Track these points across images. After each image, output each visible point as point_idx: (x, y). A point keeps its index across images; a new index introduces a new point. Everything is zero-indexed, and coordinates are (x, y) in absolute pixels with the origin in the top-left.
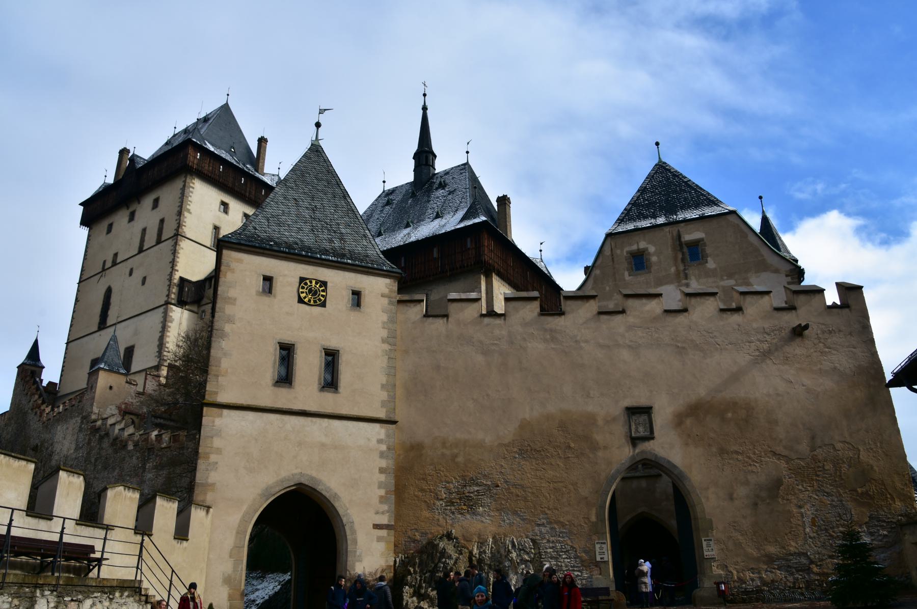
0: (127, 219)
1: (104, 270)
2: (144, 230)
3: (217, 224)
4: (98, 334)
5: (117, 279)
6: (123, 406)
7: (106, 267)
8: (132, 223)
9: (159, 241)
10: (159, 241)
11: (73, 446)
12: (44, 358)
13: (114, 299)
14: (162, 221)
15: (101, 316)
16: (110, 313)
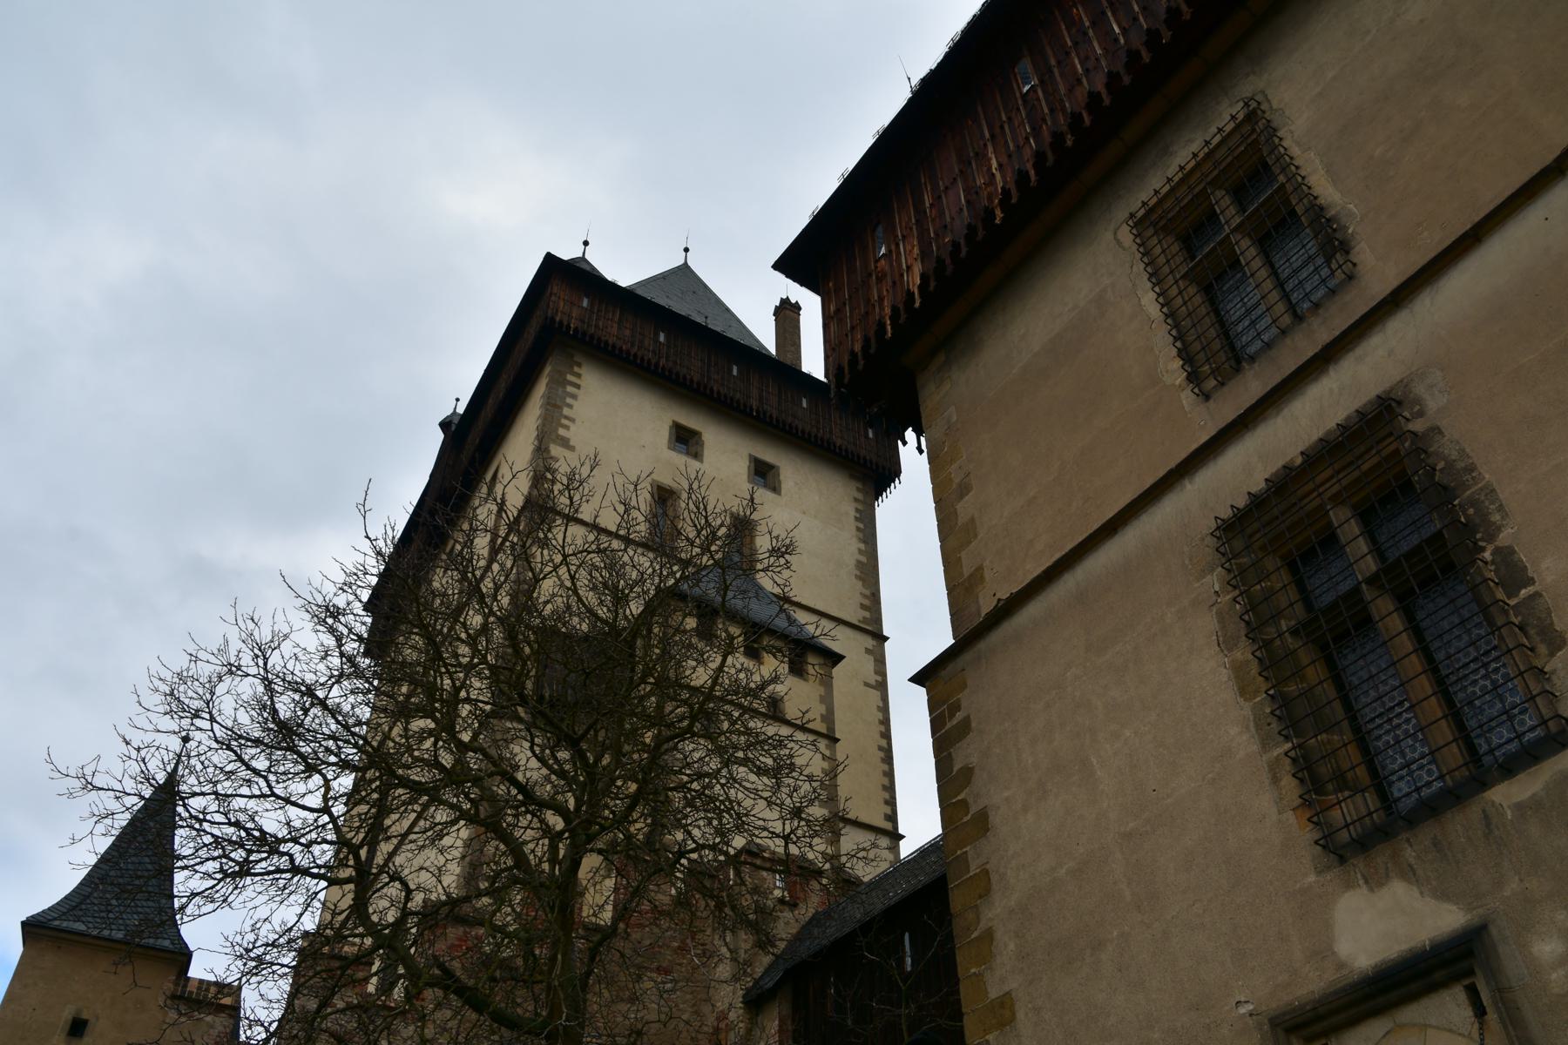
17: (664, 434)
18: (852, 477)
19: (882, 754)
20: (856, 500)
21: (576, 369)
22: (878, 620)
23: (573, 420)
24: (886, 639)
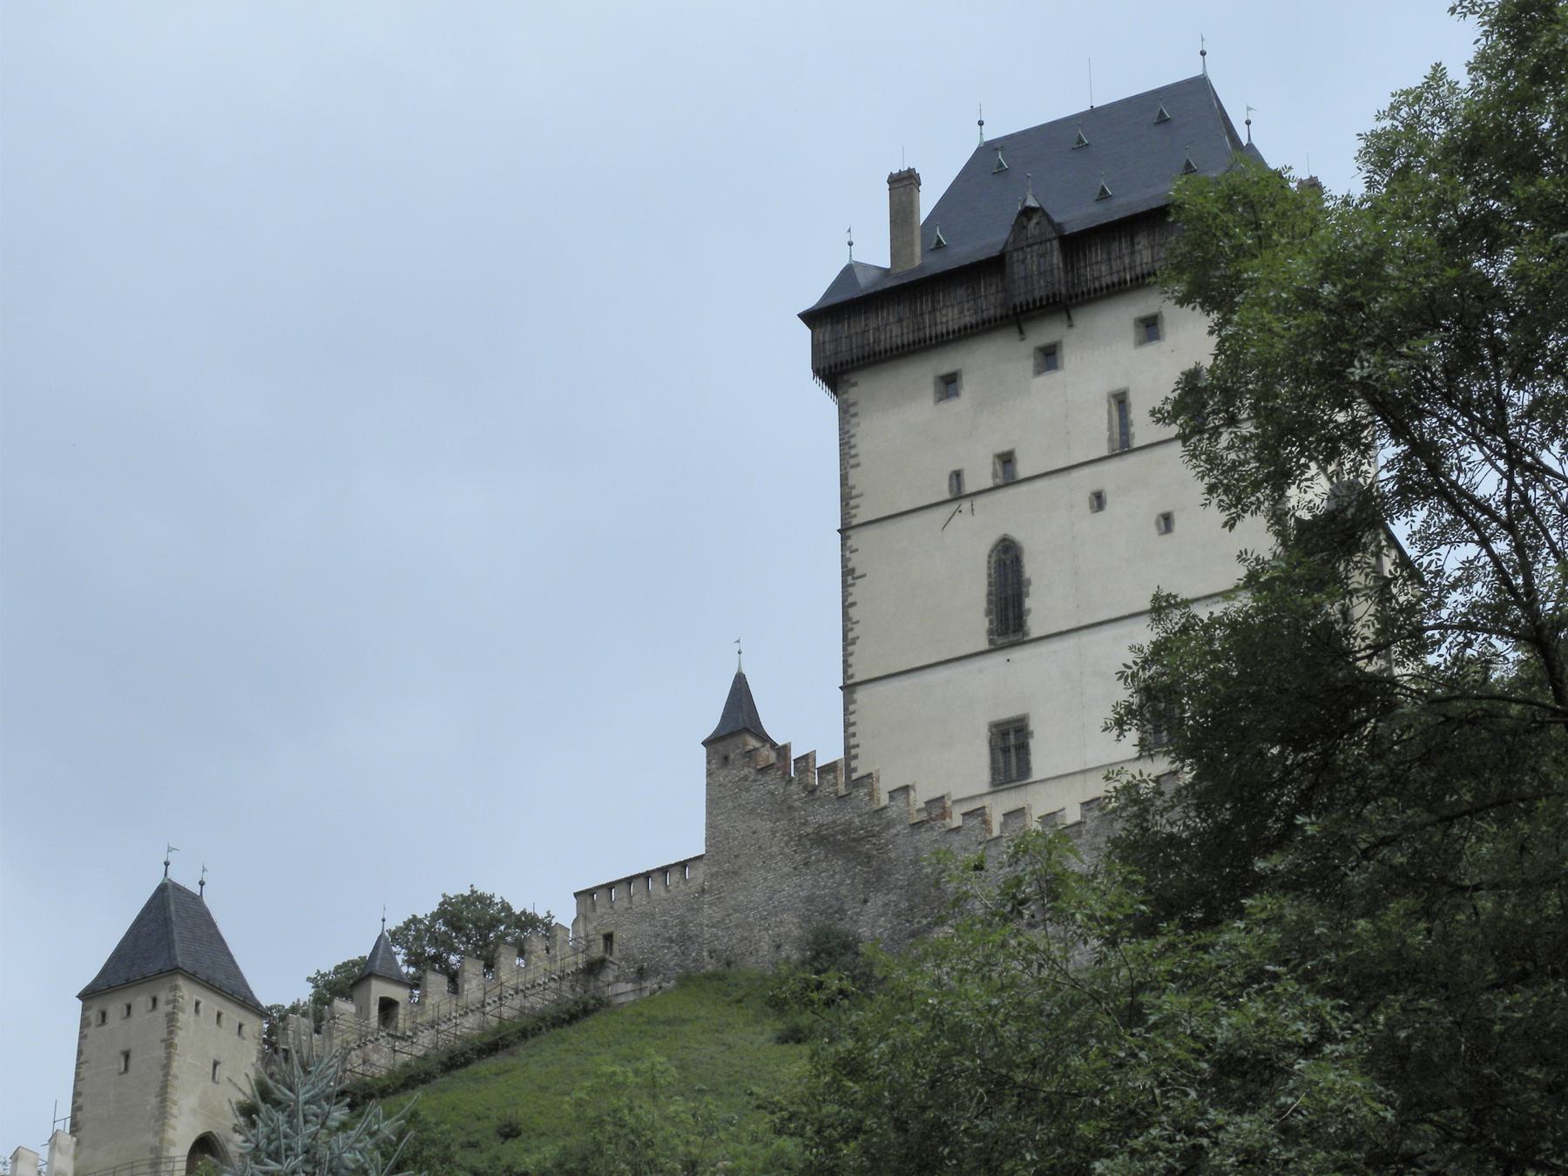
0: (1030, 364)
2: (1121, 401)
4: (998, 659)
7: (969, 488)
13: (1031, 568)
15: (988, 613)
16: (1029, 603)
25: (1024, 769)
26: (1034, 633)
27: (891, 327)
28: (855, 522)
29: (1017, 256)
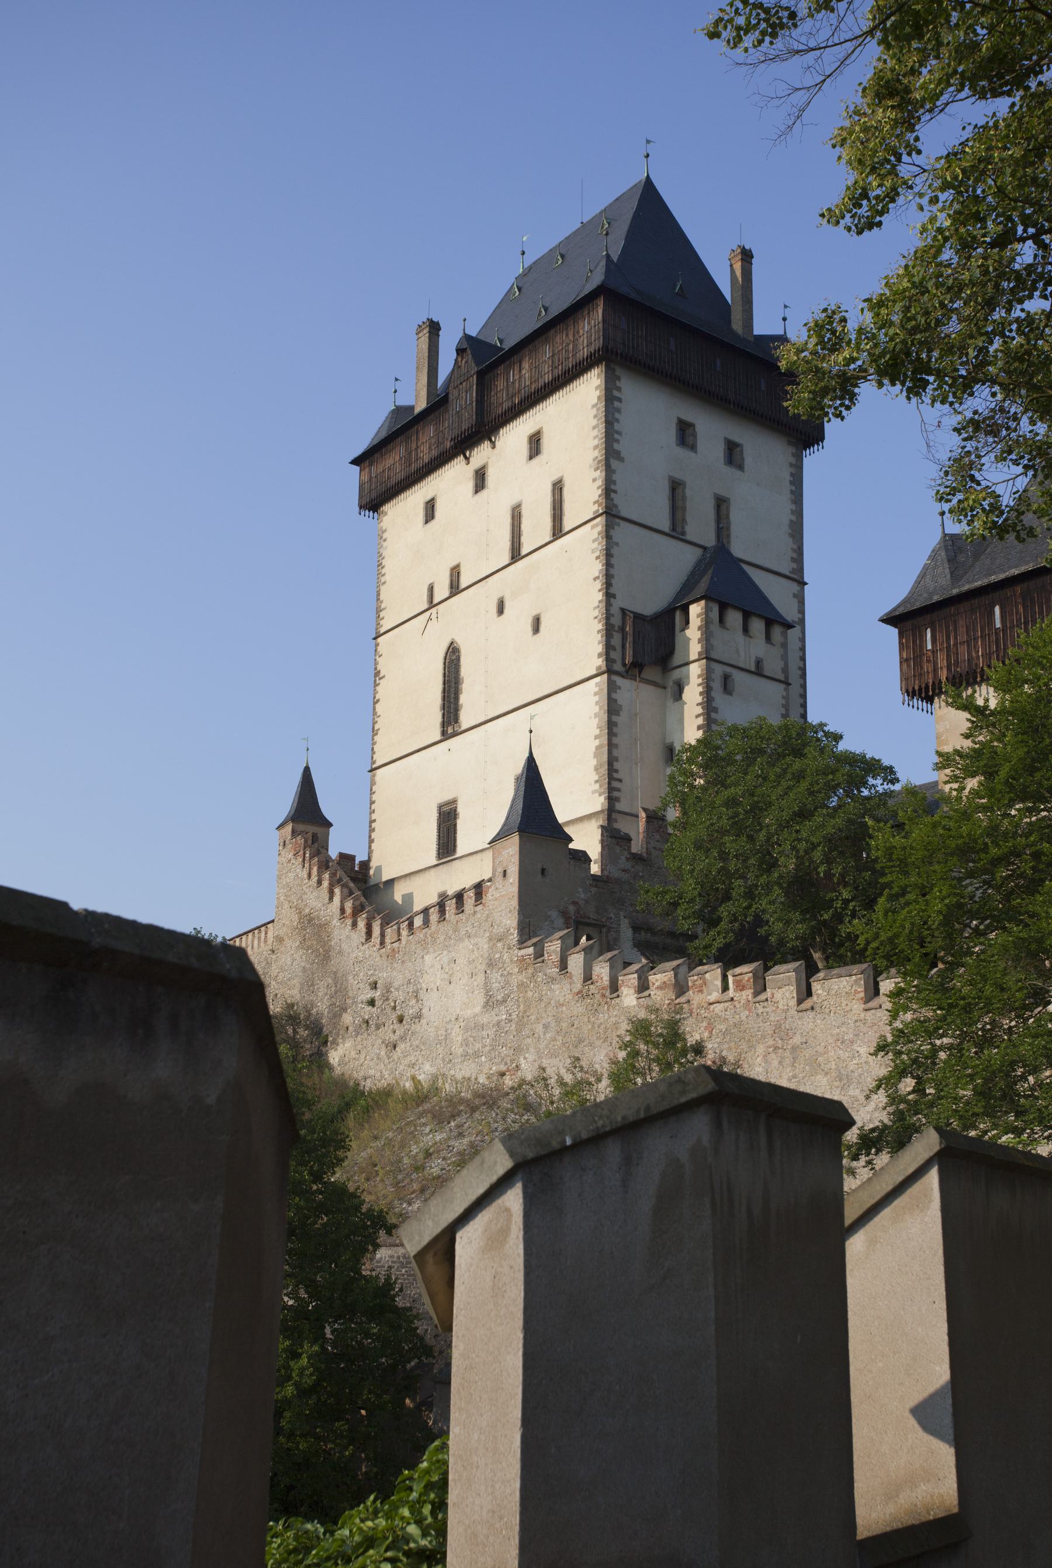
0: (470, 485)
1: (432, 605)
3: (678, 475)
5: (464, 621)
6: (572, 909)
8: (483, 494)
9: (558, 532)
10: (558, 532)
11: (481, 999)
12: (327, 807)
14: (558, 487)
16: (463, 699)
17: (671, 433)
18: (790, 443)
19: (800, 672)
20: (791, 465)
21: (618, 383)
22: (801, 570)
23: (619, 433)
24: (806, 584)
25: (454, 850)
26: (463, 728)
27: (393, 462)
28: (382, 630)
29: (455, 392)
